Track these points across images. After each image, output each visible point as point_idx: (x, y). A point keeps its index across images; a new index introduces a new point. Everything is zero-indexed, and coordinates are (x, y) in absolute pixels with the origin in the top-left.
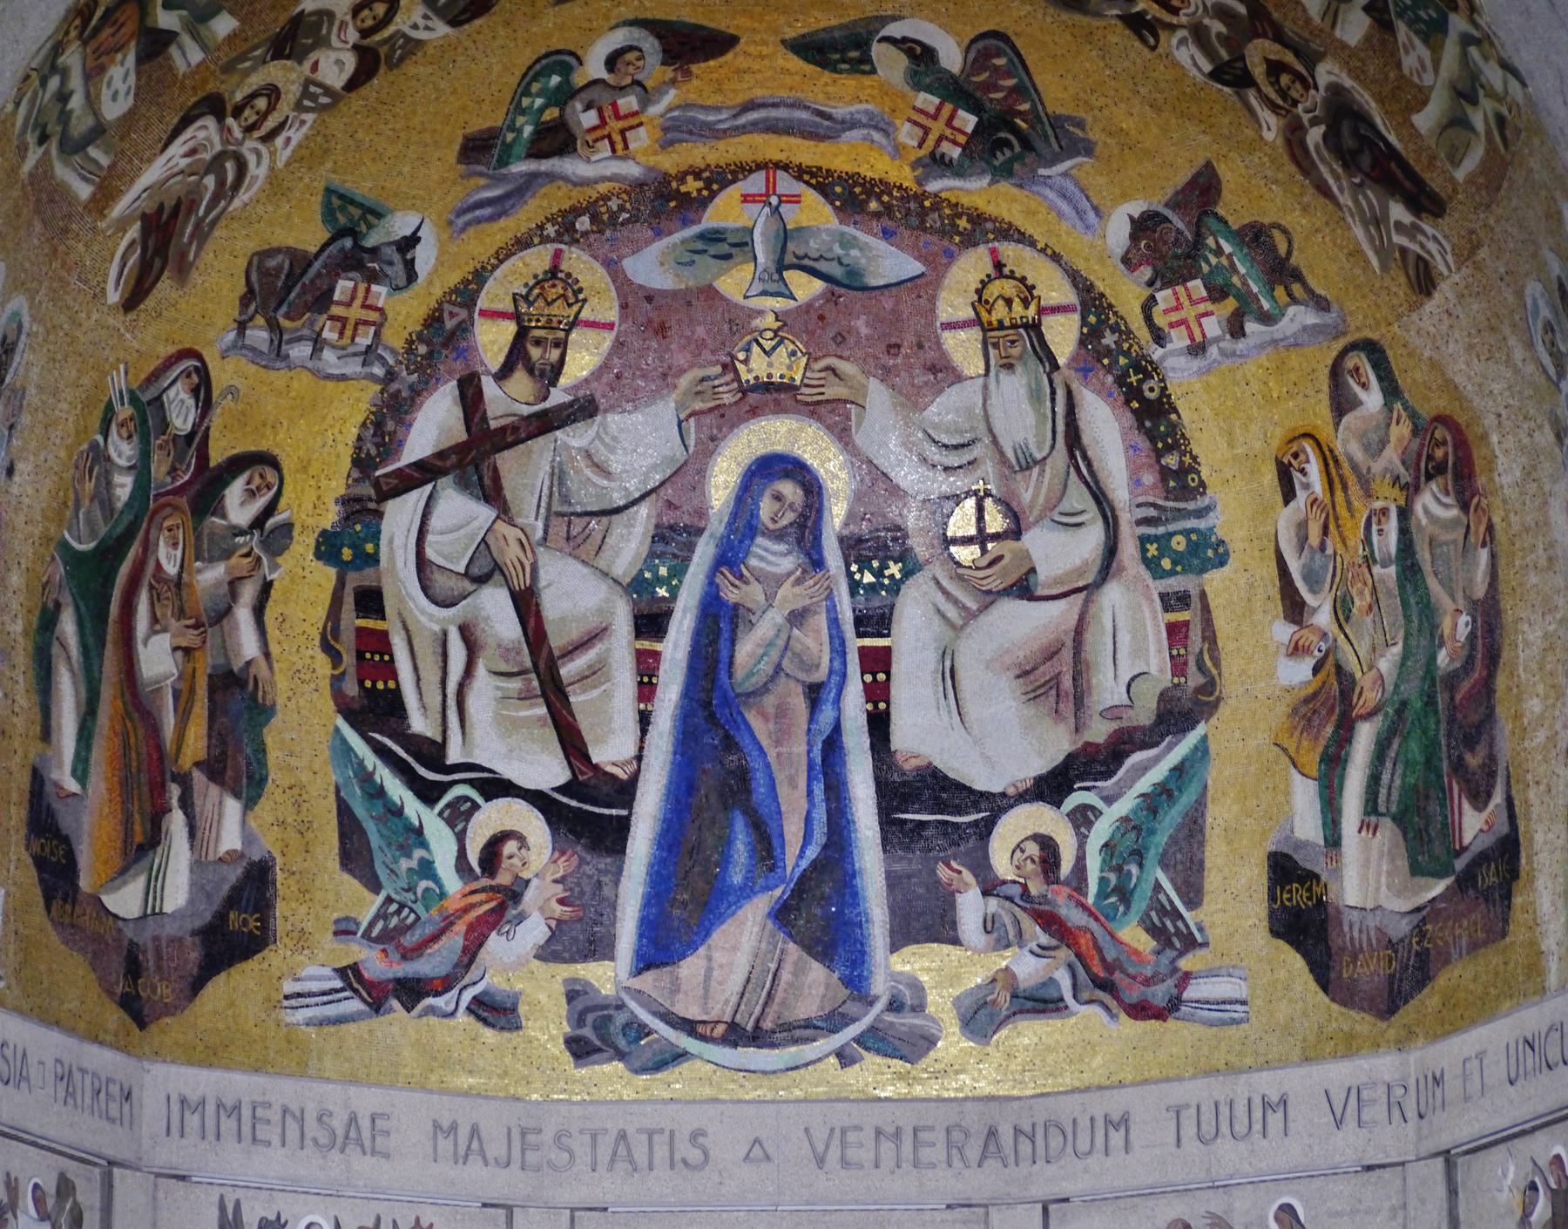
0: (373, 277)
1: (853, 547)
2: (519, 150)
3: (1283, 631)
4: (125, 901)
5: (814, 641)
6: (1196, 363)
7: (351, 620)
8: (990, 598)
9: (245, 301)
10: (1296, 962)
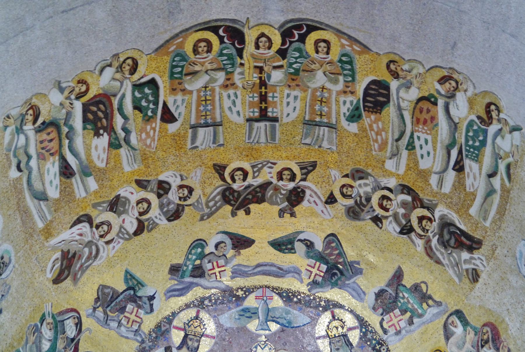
0: (139, 307)
2: (188, 273)
6: (398, 337)
9: (97, 300)
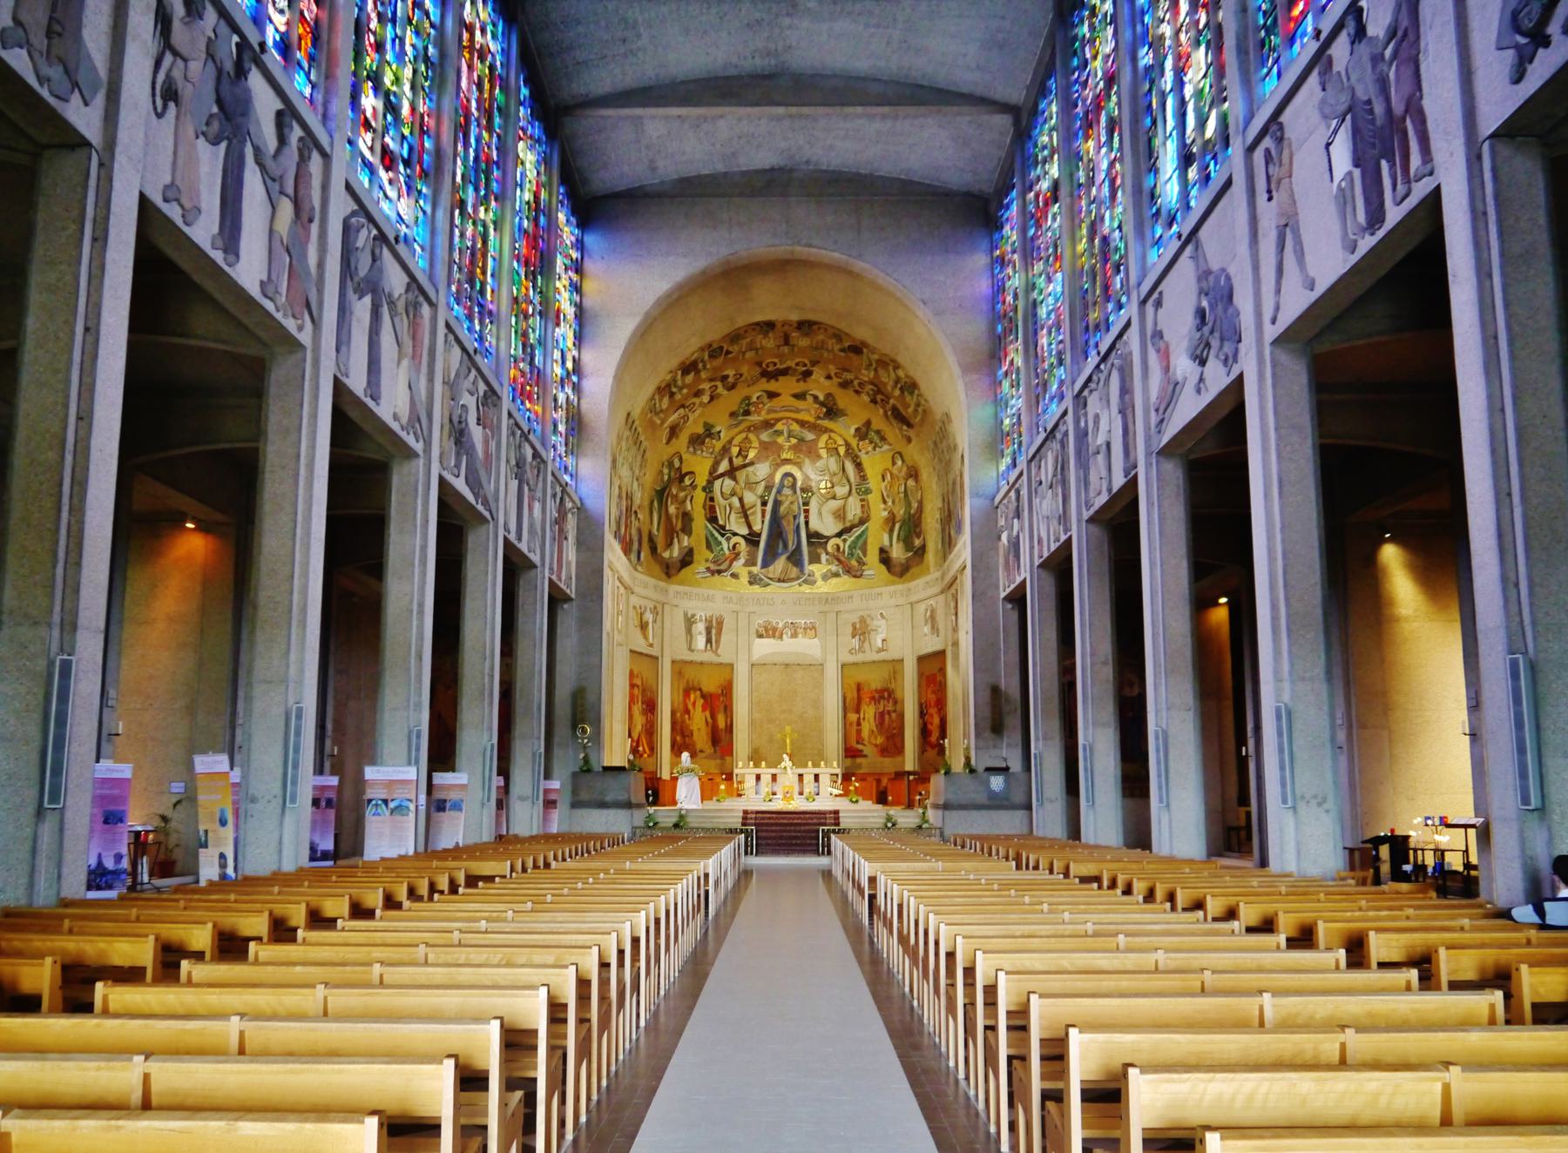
1: (803, 490)
3: (882, 506)
4: (666, 555)
5: (795, 507)
7: (708, 503)
8: (827, 500)
10: (883, 568)
